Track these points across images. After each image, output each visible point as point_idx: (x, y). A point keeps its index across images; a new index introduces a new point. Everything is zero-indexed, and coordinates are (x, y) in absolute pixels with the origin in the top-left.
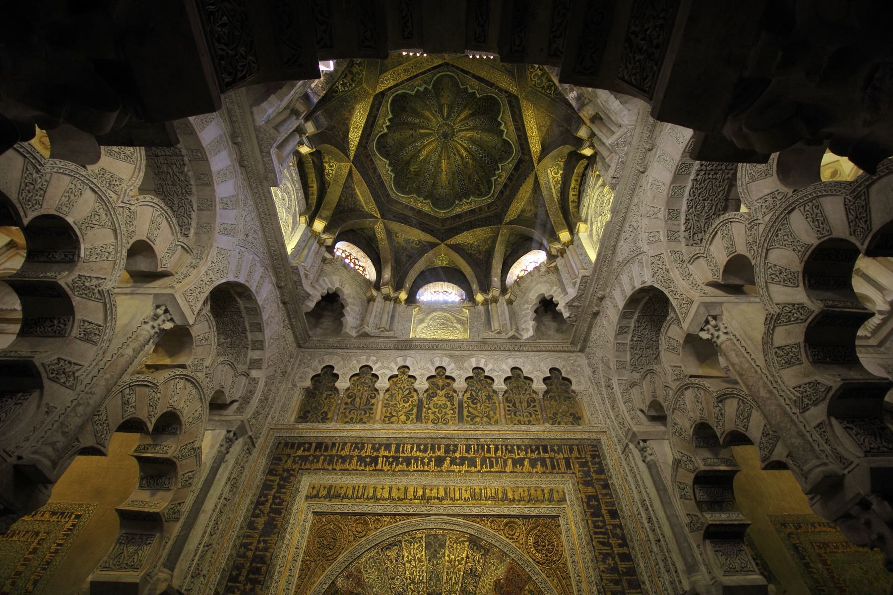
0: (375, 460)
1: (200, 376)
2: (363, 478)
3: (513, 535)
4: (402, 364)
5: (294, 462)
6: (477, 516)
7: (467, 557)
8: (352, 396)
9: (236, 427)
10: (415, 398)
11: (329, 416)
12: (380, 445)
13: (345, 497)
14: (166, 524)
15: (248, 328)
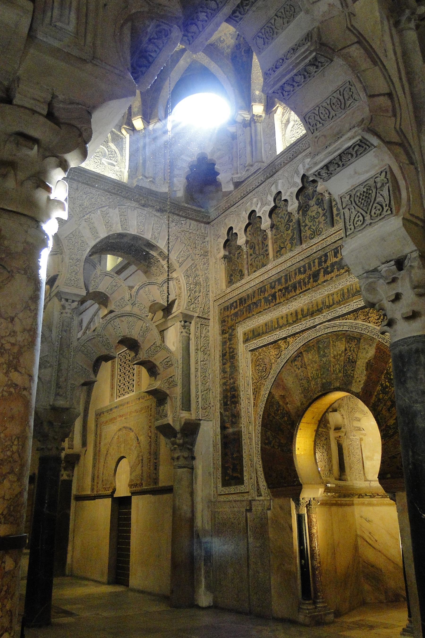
0: (274, 296)
1: (128, 309)
2: (270, 314)
3: (378, 319)
4: (275, 192)
5: (232, 320)
6: (349, 313)
7: (346, 350)
8: (253, 246)
9: (181, 318)
10: (294, 221)
11: (243, 273)
12: (275, 282)
13: (263, 333)
14: (168, 392)
15: (148, 250)
